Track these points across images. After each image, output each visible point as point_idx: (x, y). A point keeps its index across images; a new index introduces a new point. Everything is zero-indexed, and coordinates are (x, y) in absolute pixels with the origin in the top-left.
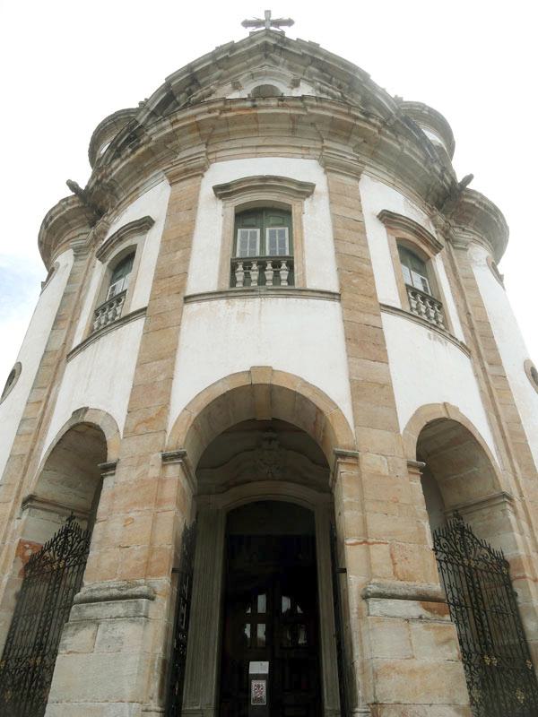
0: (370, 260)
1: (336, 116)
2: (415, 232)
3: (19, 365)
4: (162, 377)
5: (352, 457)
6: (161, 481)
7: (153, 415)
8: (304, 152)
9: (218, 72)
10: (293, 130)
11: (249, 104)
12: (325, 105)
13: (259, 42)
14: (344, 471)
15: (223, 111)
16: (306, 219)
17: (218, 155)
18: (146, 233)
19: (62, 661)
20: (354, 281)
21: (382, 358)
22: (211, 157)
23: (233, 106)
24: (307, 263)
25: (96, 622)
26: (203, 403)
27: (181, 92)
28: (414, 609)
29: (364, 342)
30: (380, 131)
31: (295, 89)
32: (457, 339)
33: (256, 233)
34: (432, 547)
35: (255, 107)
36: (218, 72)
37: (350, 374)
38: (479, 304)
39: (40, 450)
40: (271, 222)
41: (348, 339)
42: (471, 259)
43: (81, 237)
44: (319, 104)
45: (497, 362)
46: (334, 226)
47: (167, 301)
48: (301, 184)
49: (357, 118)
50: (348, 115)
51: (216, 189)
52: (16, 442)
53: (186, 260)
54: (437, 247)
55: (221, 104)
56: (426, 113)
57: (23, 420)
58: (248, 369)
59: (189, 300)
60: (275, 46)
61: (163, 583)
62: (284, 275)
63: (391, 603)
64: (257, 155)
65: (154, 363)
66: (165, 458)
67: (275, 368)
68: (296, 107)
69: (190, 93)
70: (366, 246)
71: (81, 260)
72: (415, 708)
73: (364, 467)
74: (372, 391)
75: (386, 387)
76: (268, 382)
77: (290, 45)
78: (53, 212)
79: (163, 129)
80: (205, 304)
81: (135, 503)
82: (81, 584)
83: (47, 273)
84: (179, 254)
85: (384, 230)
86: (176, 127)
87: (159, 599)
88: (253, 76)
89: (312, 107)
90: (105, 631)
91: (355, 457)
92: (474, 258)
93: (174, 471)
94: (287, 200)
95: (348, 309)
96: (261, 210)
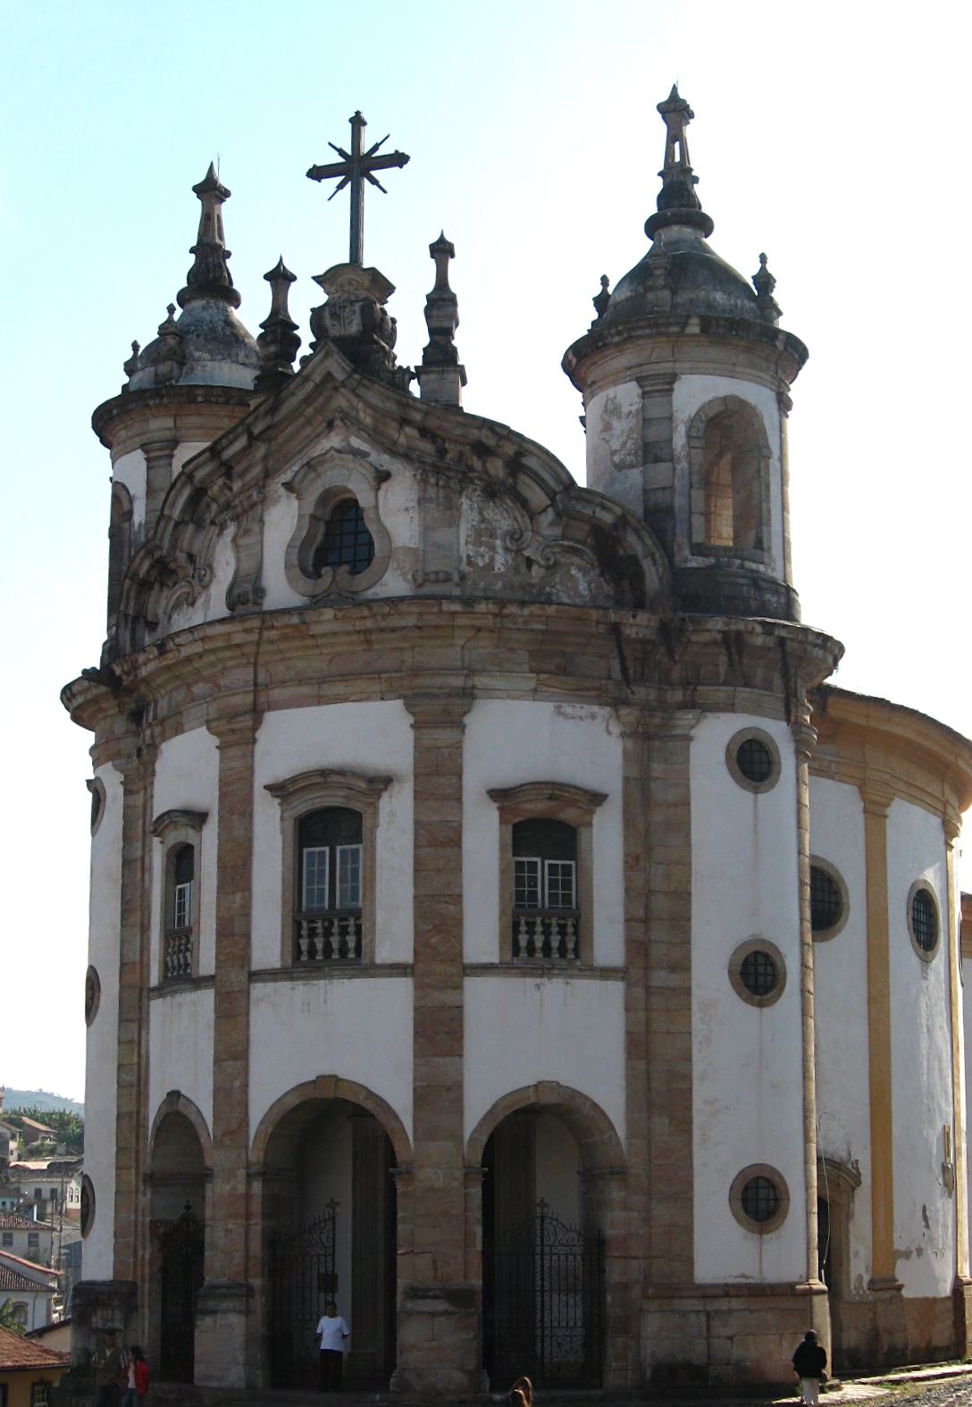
0: (460, 896)
2: (551, 798)
4: (237, 1083)
5: (410, 1175)
6: (248, 1196)
7: (234, 1126)
9: (261, 450)
10: (368, 642)
13: (317, 378)
14: (400, 1187)
16: (382, 835)
17: (276, 694)
19: (199, 1338)
20: (433, 941)
25: (213, 1312)
28: (441, 1306)
29: (439, 1032)
31: (384, 486)
33: (324, 852)
37: (415, 1080)
38: (684, 862)
39: (146, 1119)
41: (416, 1033)
45: (682, 966)
46: (416, 847)
47: (233, 975)
52: (119, 1096)
53: (246, 912)
54: (597, 798)
57: (120, 1067)
58: (314, 1078)
61: (257, 1282)
62: (351, 941)
64: (320, 700)
66: (248, 1175)
67: (341, 1076)
70: (458, 869)
74: (438, 1093)
76: (332, 1096)
80: (270, 985)
82: (204, 1279)
83: (88, 797)
84: (238, 897)
85: (495, 815)
87: (257, 1296)
93: (257, 1187)
94: (357, 806)
95: (417, 987)
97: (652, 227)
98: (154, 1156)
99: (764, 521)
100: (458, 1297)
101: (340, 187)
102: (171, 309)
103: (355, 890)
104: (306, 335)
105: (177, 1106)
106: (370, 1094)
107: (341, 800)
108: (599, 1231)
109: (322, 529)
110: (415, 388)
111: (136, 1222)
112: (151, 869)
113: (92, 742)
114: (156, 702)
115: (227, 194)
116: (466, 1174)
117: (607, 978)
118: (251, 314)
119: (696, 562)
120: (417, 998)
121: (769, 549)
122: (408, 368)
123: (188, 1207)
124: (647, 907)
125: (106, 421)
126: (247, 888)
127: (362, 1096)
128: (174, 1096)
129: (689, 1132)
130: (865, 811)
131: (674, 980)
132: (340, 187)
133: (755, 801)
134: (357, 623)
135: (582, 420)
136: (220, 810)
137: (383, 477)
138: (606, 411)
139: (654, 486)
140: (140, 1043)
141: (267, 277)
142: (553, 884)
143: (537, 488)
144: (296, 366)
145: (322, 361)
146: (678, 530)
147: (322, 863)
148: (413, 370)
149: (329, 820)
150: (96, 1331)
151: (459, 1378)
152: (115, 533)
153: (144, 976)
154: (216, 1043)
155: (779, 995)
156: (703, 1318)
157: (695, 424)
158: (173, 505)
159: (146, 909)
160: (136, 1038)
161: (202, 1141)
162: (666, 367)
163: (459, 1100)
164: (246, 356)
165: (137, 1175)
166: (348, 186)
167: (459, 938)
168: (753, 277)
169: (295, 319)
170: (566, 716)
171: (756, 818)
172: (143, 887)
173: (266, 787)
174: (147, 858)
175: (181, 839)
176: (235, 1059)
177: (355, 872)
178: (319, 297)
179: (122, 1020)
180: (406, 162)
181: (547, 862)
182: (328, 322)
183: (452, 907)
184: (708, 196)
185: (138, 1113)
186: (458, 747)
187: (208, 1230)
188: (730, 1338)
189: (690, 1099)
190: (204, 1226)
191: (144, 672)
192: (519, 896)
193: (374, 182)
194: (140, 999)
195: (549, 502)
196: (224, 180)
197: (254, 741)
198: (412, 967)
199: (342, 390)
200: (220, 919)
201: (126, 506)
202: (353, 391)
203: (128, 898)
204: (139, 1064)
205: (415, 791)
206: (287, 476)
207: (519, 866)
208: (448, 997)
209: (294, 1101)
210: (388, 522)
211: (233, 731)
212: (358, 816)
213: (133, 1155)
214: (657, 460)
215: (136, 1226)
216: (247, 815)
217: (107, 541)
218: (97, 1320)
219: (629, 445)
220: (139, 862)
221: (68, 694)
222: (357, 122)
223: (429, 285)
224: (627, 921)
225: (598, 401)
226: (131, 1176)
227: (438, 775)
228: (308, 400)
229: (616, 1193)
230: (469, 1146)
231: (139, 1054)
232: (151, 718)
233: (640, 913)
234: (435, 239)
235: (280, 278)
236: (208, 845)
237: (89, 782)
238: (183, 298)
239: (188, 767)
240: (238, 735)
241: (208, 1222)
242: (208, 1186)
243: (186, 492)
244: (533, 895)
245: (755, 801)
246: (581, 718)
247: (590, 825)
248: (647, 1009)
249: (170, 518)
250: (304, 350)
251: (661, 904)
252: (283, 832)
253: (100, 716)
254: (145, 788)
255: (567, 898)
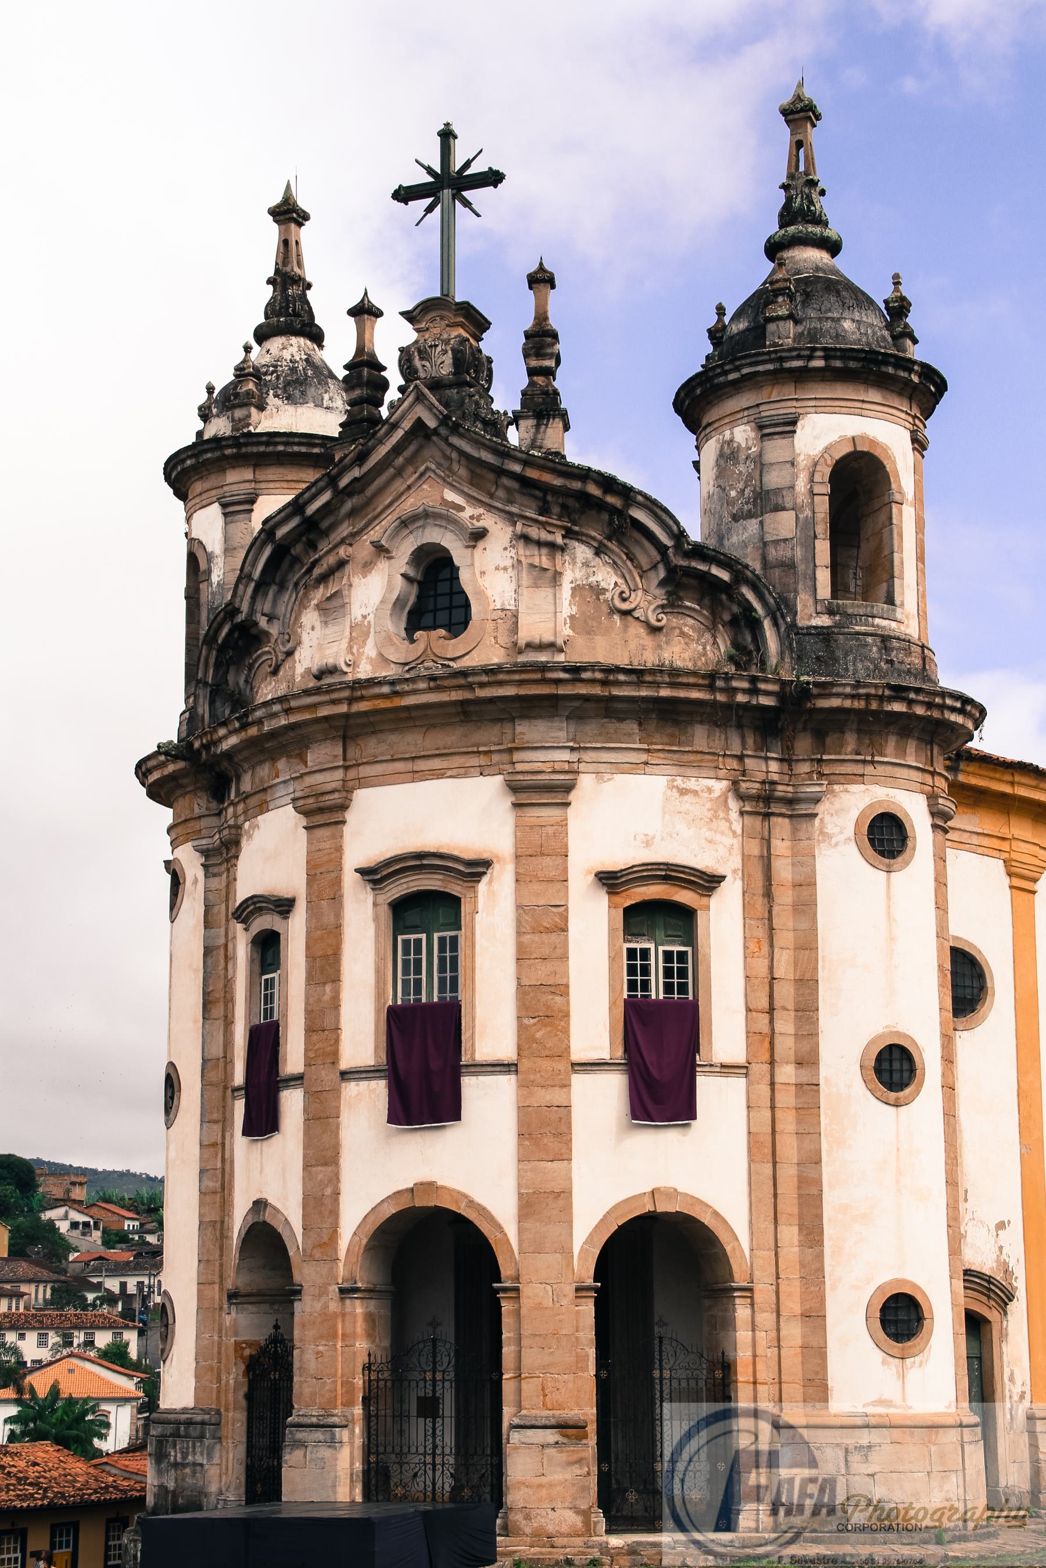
0: (567, 986)
1: (523, 691)
2: (666, 878)
3: (171, 1065)
4: (328, 1191)
7: (326, 1239)
8: (482, 760)
9: (348, 505)
11: (386, 689)
12: (501, 677)
13: (407, 425)
14: (506, 1307)
15: (351, 701)
17: (366, 771)
18: (287, 918)
20: (538, 1035)
21: (564, 1156)
22: (352, 774)
23: (364, 692)
24: (479, 1011)
25: (302, 1444)
26: (371, 1227)
27: (297, 540)
28: (551, 1436)
30: (604, 683)
31: (481, 545)
32: (711, 1065)
33: (420, 940)
34: (593, 1372)
35: (396, 693)
36: (348, 505)
37: (519, 1186)
38: (807, 946)
39: (230, 1229)
40: (441, 921)
41: (520, 1135)
42: (822, 833)
43: (204, 823)
44: (492, 679)
45: (808, 1060)
46: (519, 933)
48: (470, 863)
49: (558, 682)
50: (544, 681)
51: (362, 872)
52: (202, 1204)
53: (335, 1004)
55: (346, 694)
56: (819, 363)
57: (202, 1172)
59: (347, 1077)
60: (435, 431)
63: (530, 1432)
64: (416, 776)
65: (320, 1168)
68: (460, 687)
69: (313, 546)
70: (564, 957)
71: (215, 875)
72: (539, 1511)
73: (524, 1300)
74: (544, 1202)
75: (564, 1195)
77: (461, 436)
78: (151, 763)
79: (274, 715)
80: (363, 1084)
81: (321, 1337)
84: (328, 988)
85: (602, 899)
86: (293, 719)
88: (405, 523)
89: (482, 685)
90: (311, 1453)
91: (517, 1290)
92: (830, 829)
94: (455, 888)
95: (522, 1085)
96: (426, 900)
97: (773, 249)
98: (239, 1269)
99: (896, 574)
100: (568, 1428)
101: (429, 209)
102: (247, 349)
103: (454, 981)
104: (394, 377)
105: (264, 1215)
106: (471, 1203)
107: (439, 883)
108: (723, 1353)
109: (414, 590)
110: (513, 436)
111: (220, 1344)
112: (234, 958)
113: (169, 820)
114: (238, 778)
115: (306, 217)
116: (578, 1290)
117: (727, 1075)
118: (337, 353)
119: (825, 621)
120: (520, 1097)
121: (902, 605)
122: (506, 413)
123: (276, 1327)
124: (771, 997)
125: (184, 473)
126: (335, 979)
127: (463, 1205)
128: (260, 1205)
129: (820, 1243)
130: (1011, 887)
131: (805, 1076)
132: (429, 209)
133: (888, 879)
134: (453, 693)
135: (696, 465)
136: (308, 894)
137: (479, 535)
138: (721, 455)
139: (775, 538)
140: (223, 1145)
141: (352, 312)
142: (668, 973)
143: (647, 544)
144: (384, 412)
145: (411, 406)
146: (800, 587)
147: (418, 951)
148: (510, 415)
149: (426, 900)
150: (176, 1465)
151: (571, 1519)
152: (192, 596)
153: (228, 1074)
154: (306, 1147)
155: (918, 1092)
156: (841, 1454)
157: (818, 468)
158: (254, 565)
159: (229, 1001)
160: (219, 1141)
161: (291, 1254)
162: (785, 409)
163: (567, 1209)
164: (331, 399)
165: (221, 1289)
166: (438, 209)
167: (566, 1031)
168: (886, 302)
169: (382, 359)
170: (683, 792)
171: (889, 897)
172: (226, 977)
173: (357, 870)
174: (230, 946)
175: (267, 926)
176: (326, 1164)
177: (454, 960)
178: (408, 335)
179: (205, 1119)
180: (501, 181)
181: (661, 949)
182: (417, 363)
183: (558, 999)
184: (837, 212)
185: (222, 1222)
186: (563, 824)
187: (296, 1352)
188: (873, 1475)
189: (820, 1206)
190: (293, 1348)
191: (225, 746)
192: (632, 985)
193: (467, 204)
194: (224, 1097)
195: (659, 558)
196: (303, 202)
197: (344, 822)
198: (516, 1065)
199: (435, 438)
200: (308, 1012)
201: (203, 565)
202: (446, 440)
203: (211, 988)
204: (223, 1169)
205: (517, 873)
206: (374, 534)
207: (631, 953)
208: (555, 1096)
209: (391, 1210)
210: (484, 582)
211: (321, 810)
212: (455, 902)
213: (217, 1269)
214: (779, 508)
215: (219, 1348)
216: (336, 899)
217: (185, 601)
218: (175, 1455)
219: (747, 491)
220: (222, 951)
221: (142, 769)
222: (447, 135)
223: (528, 323)
224: (748, 1010)
225: (711, 448)
226: (215, 1291)
227: (543, 855)
228: (397, 450)
229: (742, 1312)
230: (580, 1258)
231: (223, 1160)
232: (232, 797)
233: (764, 1003)
234: (534, 267)
235: (364, 312)
236: (295, 934)
237: (168, 864)
238: (262, 335)
239: (273, 851)
240: (324, 814)
241: (297, 1343)
242: (296, 1304)
243: (267, 552)
244: (645, 986)
245: (888, 879)
246: (695, 793)
247: (708, 908)
248: (773, 1108)
249: (249, 577)
250: (392, 395)
251: (785, 994)
252: (376, 919)
253: (179, 792)
254: (228, 870)
255: (683, 988)
